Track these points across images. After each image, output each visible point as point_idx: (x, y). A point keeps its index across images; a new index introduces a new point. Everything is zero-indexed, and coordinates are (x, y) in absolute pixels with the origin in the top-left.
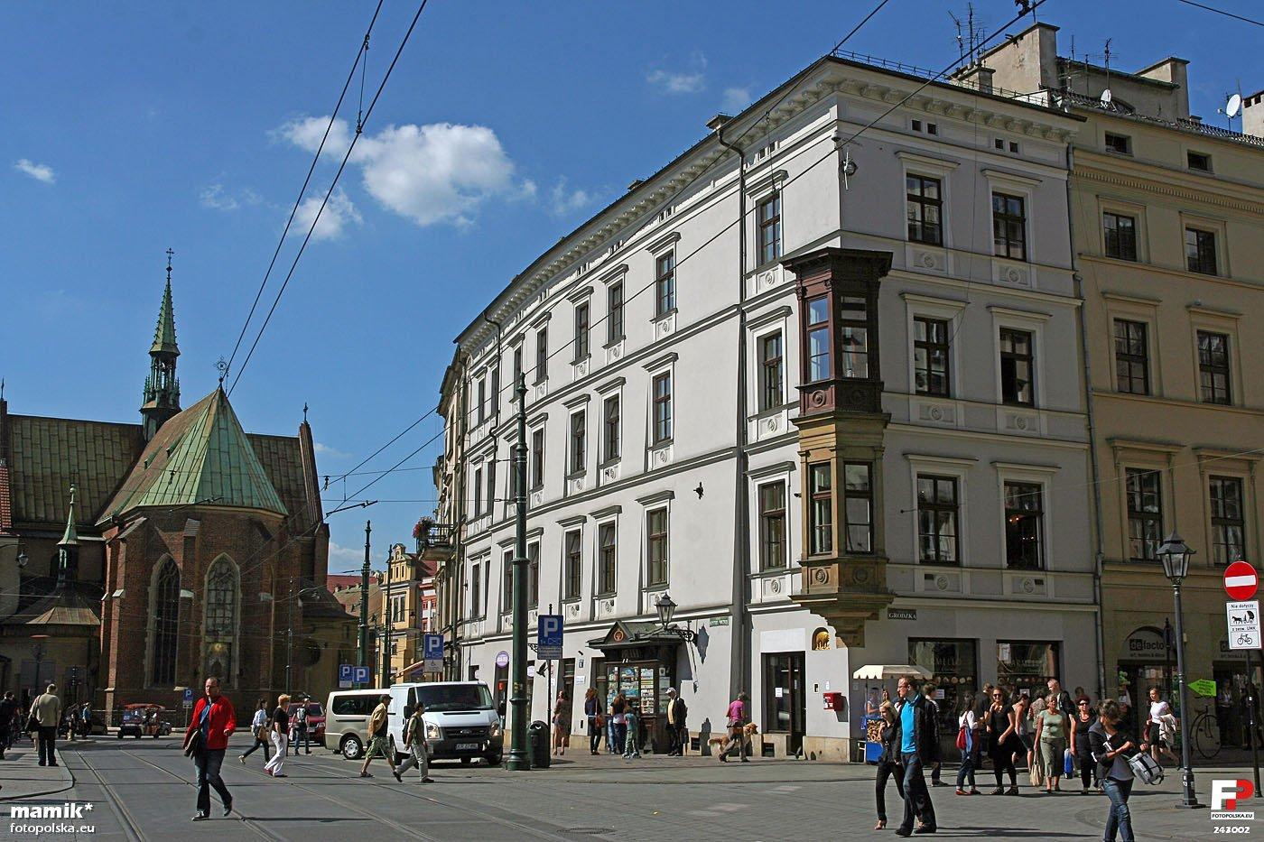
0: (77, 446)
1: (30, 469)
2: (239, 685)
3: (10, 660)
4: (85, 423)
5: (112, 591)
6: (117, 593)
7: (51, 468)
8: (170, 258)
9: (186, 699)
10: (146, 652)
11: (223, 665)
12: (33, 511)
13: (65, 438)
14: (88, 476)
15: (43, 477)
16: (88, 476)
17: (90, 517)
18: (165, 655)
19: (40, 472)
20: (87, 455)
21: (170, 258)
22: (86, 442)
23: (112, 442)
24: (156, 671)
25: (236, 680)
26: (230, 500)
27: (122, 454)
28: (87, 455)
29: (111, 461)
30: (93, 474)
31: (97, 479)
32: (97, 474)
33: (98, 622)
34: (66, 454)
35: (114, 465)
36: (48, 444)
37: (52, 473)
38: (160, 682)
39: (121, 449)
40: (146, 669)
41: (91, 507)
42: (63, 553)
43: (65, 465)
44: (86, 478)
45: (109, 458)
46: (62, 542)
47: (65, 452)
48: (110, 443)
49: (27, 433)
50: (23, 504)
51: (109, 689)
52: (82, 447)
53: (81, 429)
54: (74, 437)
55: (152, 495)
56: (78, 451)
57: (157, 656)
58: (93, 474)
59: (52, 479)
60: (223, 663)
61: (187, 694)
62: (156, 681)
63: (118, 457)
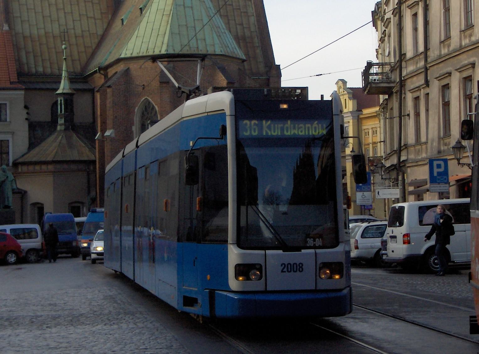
0: (64, 9)
3: (26, 192)
5: (103, 131)
6: (108, 133)
7: (44, 29)
12: (34, 66)
14: (75, 34)
15: (39, 36)
16: (75, 34)
17: (79, 67)
19: (36, 32)
20: (72, 16)
22: (71, 5)
23: (93, 3)
26: (195, 49)
27: (102, 13)
28: (72, 16)
29: (93, 21)
30: (79, 32)
31: (83, 36)
32: (82, 31)
33: (92, 158)
35: (96, 23)
37: (46, 33)
39: (101, 10)
41: (79, 60)
42: (61, 101)
43: (56, 25)
45: (91, 18)
46: (59, 91)
48: (90, 4)
50: (24, 60)
52: (68, 9)
55: (130, 45)
56: (65, 13)
58: (79, 32)
59: (46, 37)
63: (98, 16)
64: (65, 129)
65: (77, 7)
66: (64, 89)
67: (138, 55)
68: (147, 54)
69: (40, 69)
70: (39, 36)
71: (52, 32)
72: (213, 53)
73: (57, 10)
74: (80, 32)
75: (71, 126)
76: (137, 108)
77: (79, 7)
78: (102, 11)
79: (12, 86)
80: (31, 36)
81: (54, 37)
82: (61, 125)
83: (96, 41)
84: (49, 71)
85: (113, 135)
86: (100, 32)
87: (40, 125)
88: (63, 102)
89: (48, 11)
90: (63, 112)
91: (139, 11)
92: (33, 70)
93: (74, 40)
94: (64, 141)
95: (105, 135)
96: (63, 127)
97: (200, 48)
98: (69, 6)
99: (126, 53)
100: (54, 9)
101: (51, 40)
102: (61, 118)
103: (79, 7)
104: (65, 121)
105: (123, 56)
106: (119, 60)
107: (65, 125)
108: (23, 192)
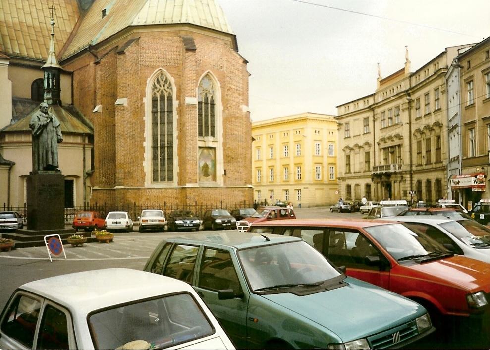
2: (225, 182)
3: (14, 164)
10: (145, 155)
11: (210, 166)
14: (46, 27)
15: (13, 24)
16: (46, 27)
19: (11, 20)
20: (43, 13)
22: (42, 4)
23: (60, 7)
24: (155, 171)
25: (222, 179)
26: (212, 25)
27: (69, 16)
34: (29, 10)
35: (64, 23)
37: (20, 22)
39: (68, 13)
42: (48, 75)
44: (45, 28)
47: (27, 10)
51: (117, 187)
57: (155, 157)
60: (209, 164)
62: (155, 179)
63: (66, 16)
66: (51, 63)
67: (153, 24)
68: (165, 23)
69: (17, 51)
71: (26, 23)
72: (227, 32)
73: (29, 5)
75: (56, 101)
76: (149, 79)
78: (70, 15)
80: (5, 22)
81: (28, 27)
82: (48, 99)
83: (67, 37)
86: (69, 30)
87: (23, 101)
90: (50, 87)
92: (11, 51)
95: (116, 104)
96: (51, 101)
97: (216, 25)
98: (41, 5)
99: (138, 20)
101: (26, 29)
102: (48, 92)
104: (52, 95)
106: (130, 28)
107: (52, 100)
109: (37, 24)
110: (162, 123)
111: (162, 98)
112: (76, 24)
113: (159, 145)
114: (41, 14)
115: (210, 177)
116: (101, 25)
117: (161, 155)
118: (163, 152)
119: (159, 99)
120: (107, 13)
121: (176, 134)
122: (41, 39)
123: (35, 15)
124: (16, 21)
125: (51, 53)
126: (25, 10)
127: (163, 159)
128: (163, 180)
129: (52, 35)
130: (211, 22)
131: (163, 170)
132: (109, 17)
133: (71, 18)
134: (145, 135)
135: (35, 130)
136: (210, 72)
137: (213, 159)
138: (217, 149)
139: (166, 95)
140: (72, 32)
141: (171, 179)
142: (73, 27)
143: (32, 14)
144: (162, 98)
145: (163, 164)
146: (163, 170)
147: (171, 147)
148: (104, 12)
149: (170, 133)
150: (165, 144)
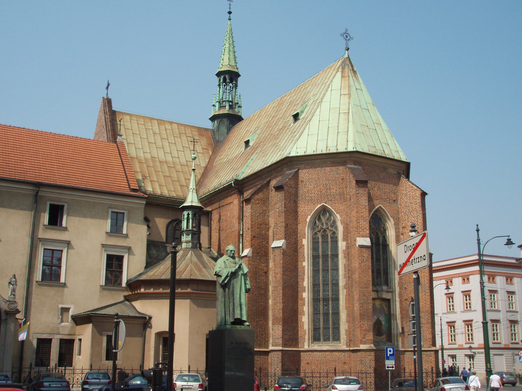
1: (135, 152)
4: (171, 123)
8: (230, 5)
9: (388, 358)
10: (306, 309)
11: (383, 323)
13: (157, 131)
14: (180, 162)
16: (180, 162)
18: (326, 314)
19: (142, 155)
20: (176, 146)
21: (230, 5)
24: (316, 329)
34: (161, 144)
36: (145, 135)
38: (322, 339)
40: (306, 327)
42: (188, 215)
47: (159, 143)
49: (128, 125)
53: (168, 126)
54: (165, 132)
57: (316, 312)
58: (183, 161)
60: (383, 319)
61: (389, 353)
62: (316, 338)
64: (192, 248)
65: (180, 140)
66: (192, 202)
68: (328, 152)
70: (146, 159)
72: (399, 159)
74: (185, 162)
77: (181, 139)
79: (132, 193)
82: (187, 242)
84: (158, 192)
85: (284, 247)
88: (190, 216)
89: (153, 138)
91: (244, 145)
93: (180, 167)
94: (195, 259)
100: (158, 137)
101: (158, 164)
103: (181, 139)
104: (192, 237)
105: (293, 154)
107: (193, 243)
108: (148, 318)
109: (169, 159)
110: (325, 270)
111: (325, 237)
112: (211, 157)
113: (321, 296)
114: (173, 147)
115: (384, 336)
116: (245, 158)
117: (324, 308)
118: (326, 305)
119: (320, 240)
120: (251, 144)
121: (342, 282)
122: (174, 175)
123: (167, 150)
124: (148, 156)
125: (191, 190)
126: (157, 144)
127: (326, 314)
128: (327, 339)
129: (194, 170)
130: (381, 149)
131: (326, 328)
132: (255, 148)
133: (205, 151)
134: (305, 284)
135: (223, 278)
136: (382, 206)
137: (387, 313)
138: (391, 300)
139: (329, 234)
140: (207, 166)
141: (337, 338)
142: (207, 161)
143: (164, 147)
144: (325, 237)
145: (326, 321)
146: (326, 328)
147: (336, 299)
148: (247, 143)
149: (334, 282)
150: (328, 295)
